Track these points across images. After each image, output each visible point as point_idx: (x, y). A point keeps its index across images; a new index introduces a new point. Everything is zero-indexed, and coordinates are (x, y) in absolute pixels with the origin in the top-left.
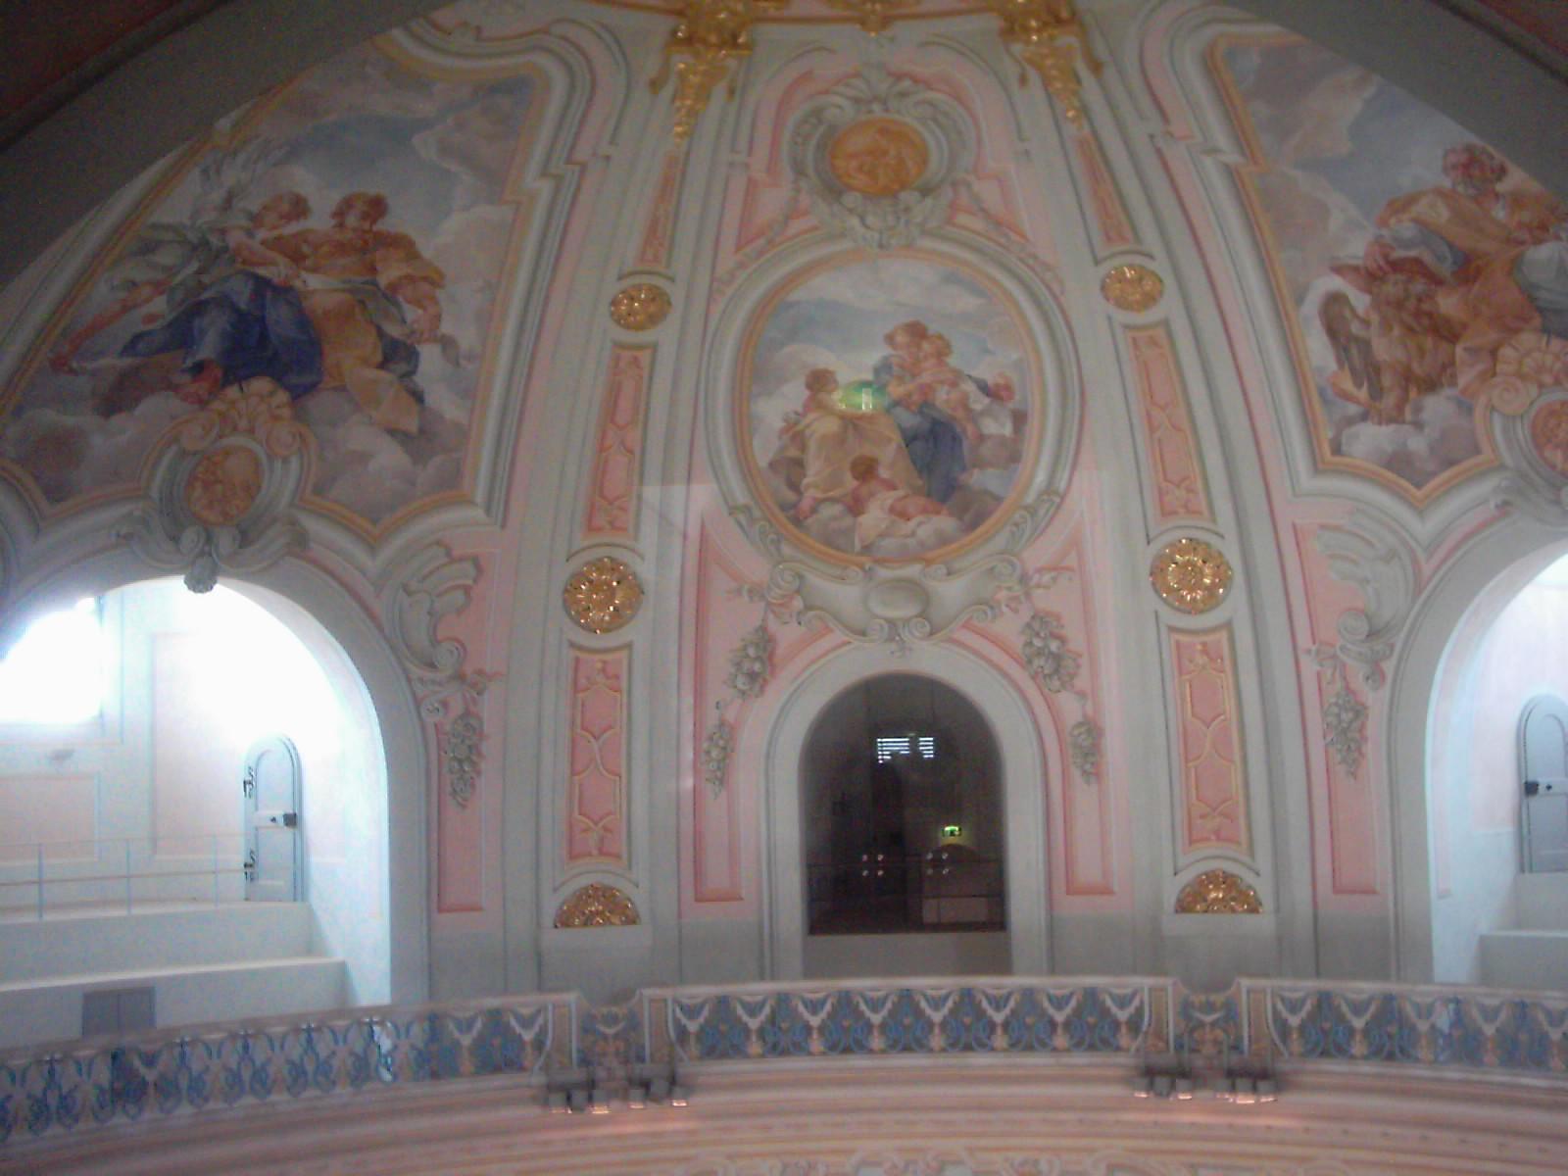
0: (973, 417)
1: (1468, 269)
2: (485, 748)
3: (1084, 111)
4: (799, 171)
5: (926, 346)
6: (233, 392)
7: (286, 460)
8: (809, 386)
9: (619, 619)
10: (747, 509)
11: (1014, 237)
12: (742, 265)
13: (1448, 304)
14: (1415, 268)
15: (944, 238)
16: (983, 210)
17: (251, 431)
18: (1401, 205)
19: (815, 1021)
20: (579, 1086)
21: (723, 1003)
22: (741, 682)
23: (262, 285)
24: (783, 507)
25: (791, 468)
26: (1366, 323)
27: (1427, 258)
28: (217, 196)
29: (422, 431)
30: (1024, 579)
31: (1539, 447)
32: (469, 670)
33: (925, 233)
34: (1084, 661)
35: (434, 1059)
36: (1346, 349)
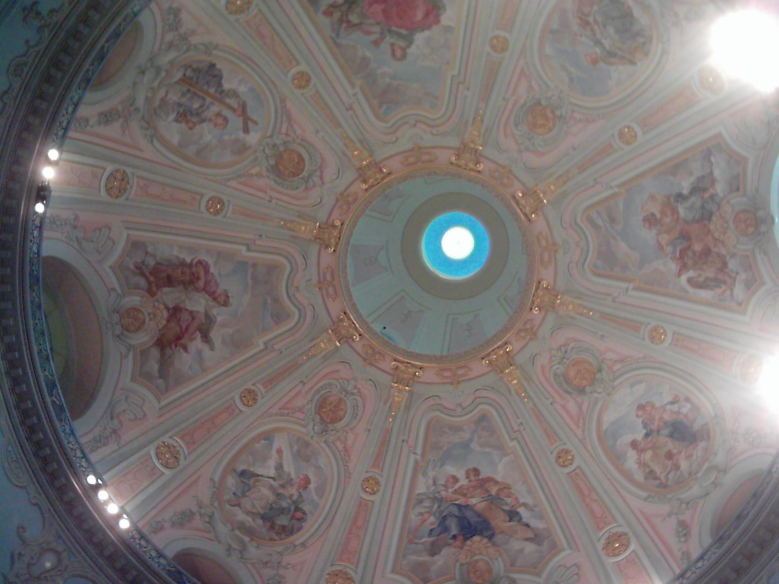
0: (678, 413)
4: (570, 393)
5: (648, 409)
6: (468, 542)
7: (497, 559)
8: (634, 449)
10: (649, 496)
11: (629, 359)
13: (697, 247)
14: (683, 253)
16: (616, 361)
17: (481, 554)
18: (660, 247)
22: (683, 539)
25: (651, 474)
26: (700, 275)
28: (431, 481)
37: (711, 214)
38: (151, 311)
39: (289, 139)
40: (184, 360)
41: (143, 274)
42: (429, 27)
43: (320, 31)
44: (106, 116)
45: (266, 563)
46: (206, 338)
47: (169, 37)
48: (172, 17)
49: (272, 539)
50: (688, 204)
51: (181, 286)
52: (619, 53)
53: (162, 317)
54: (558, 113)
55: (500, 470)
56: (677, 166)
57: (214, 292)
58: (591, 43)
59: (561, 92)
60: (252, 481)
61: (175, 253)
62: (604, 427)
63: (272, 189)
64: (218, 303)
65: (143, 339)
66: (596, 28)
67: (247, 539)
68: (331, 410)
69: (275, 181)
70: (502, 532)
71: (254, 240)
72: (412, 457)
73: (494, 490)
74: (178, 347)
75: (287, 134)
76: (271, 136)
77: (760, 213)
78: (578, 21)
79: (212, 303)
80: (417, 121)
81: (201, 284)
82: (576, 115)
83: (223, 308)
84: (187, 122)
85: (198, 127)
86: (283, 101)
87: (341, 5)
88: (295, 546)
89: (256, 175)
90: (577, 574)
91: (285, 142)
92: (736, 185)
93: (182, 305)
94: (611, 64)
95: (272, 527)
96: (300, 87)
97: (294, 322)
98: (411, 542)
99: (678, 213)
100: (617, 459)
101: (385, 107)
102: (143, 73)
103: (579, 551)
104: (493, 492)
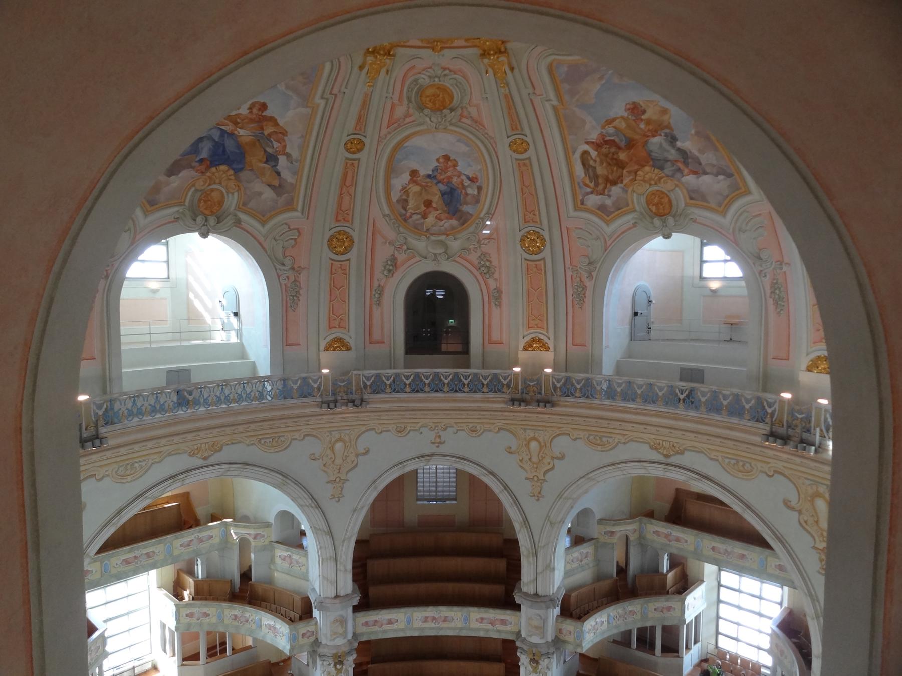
0: (464, 187)
1: (631, 144)
2: (301, 292)
3: (507, 84)
4: (410, 101)
5: (450, 163)
6: (214, 170)
7: (233, 194)
9: (347, 251)
12: (389, 133)
13: (623, 156)
14: (612, 143)
15: (457, 126)
17: (220, 183)
18: (610, 122)
19: (408, 382)
20: (331, 401)
21: (378, 376)
22: (386, 273)
23: (223, 131)
24: (401, 216)
25: (404, 202)
26: (595, 161)
27: (617, 140)
29: (280, 186)
30: (479, 242)
31: (648, 204)
32: (296, 267)
33: (451, 124)
34: (497, 269)
35: (285, 393)
36: (588, 170)
37: (662, 168)
50: (666, 145)
70: (252, 170)
77: (671, 221)
92: (696, 197)
99: (654, 136)
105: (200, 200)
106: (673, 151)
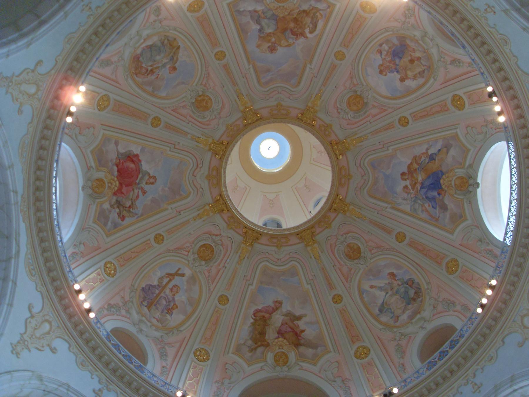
0: (388, 52)
1: (284, 31)
6: (443, 187)
7: (456, 172)
10: (434, 78)
13: (292, 25)
14: (293, 33)
17: (451, 181)
18: (289, 46)
22: (462, 65)
25: (421, 74)
26: (309, 26)
27: (290, 34)
28: (404, 202)
33: (363, 85)
37: (273, 15)
38: (278, 348)
39: (191, 250)
40: (309, 333)
41: (256, 349)
42: (140, 161)
43: (132, 224)
44: (162, 356)
45: (434, 307)
46: (299, 318)
47: (123, 312)
48: (112, 309)
49: (421, 301)
51: (267, 327)
52: (171, 55)
53: (282, 341)
54: (201, 93)
55: (404, 161)
56: (242, 31)
57: (273, 309)
58: (163, 69)
59: (189, 90)
60: (386, 307)
61: (247, 328)
62: (390, 95)
63: (219, 264)
64: (279, 307)
65: (292, 356)
66: (155, 66)
67: (418, 316)
68: (353, 252)
69: (215, 263)
70: (441, 166)
71: (247, 280)
72: (388, 210)
73: (415, 166)
74: (302, 335)
75: (188, 252)
76: (189, 261)
78: (150, 75)
79: (279, 312)
80: (193, 175)
81: (267, 315)
82: (204, 83)
83: (283, 305)
84: (173, 308)
85: (176, 303)
86: (169, 251)
87: (120, 210)
88: (428, 289)
89: (209, 273)
90: (472, 128)
91: (193, 254)
93: (277, 329)
94: (177, 59)
95: (414, 299)
96: (163, 240)
97: (299, 266)
98: (437, 220)
99: (270, 33)
100: (409, 92)
101: (182, 193)
102: (141, 331)
103: (458, 124)
104: (417, 167)
105: (460, 190)
106: (263, 23)
